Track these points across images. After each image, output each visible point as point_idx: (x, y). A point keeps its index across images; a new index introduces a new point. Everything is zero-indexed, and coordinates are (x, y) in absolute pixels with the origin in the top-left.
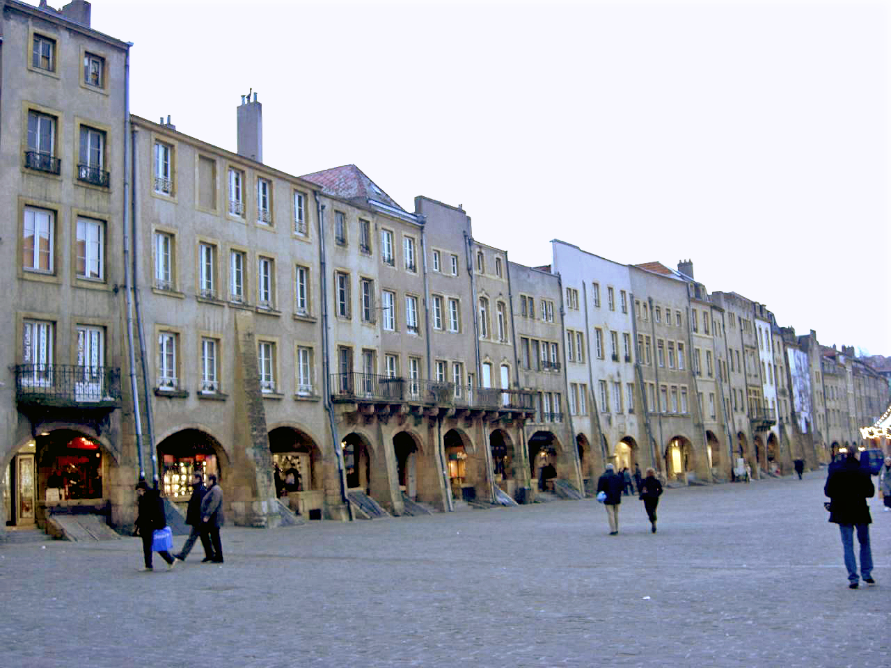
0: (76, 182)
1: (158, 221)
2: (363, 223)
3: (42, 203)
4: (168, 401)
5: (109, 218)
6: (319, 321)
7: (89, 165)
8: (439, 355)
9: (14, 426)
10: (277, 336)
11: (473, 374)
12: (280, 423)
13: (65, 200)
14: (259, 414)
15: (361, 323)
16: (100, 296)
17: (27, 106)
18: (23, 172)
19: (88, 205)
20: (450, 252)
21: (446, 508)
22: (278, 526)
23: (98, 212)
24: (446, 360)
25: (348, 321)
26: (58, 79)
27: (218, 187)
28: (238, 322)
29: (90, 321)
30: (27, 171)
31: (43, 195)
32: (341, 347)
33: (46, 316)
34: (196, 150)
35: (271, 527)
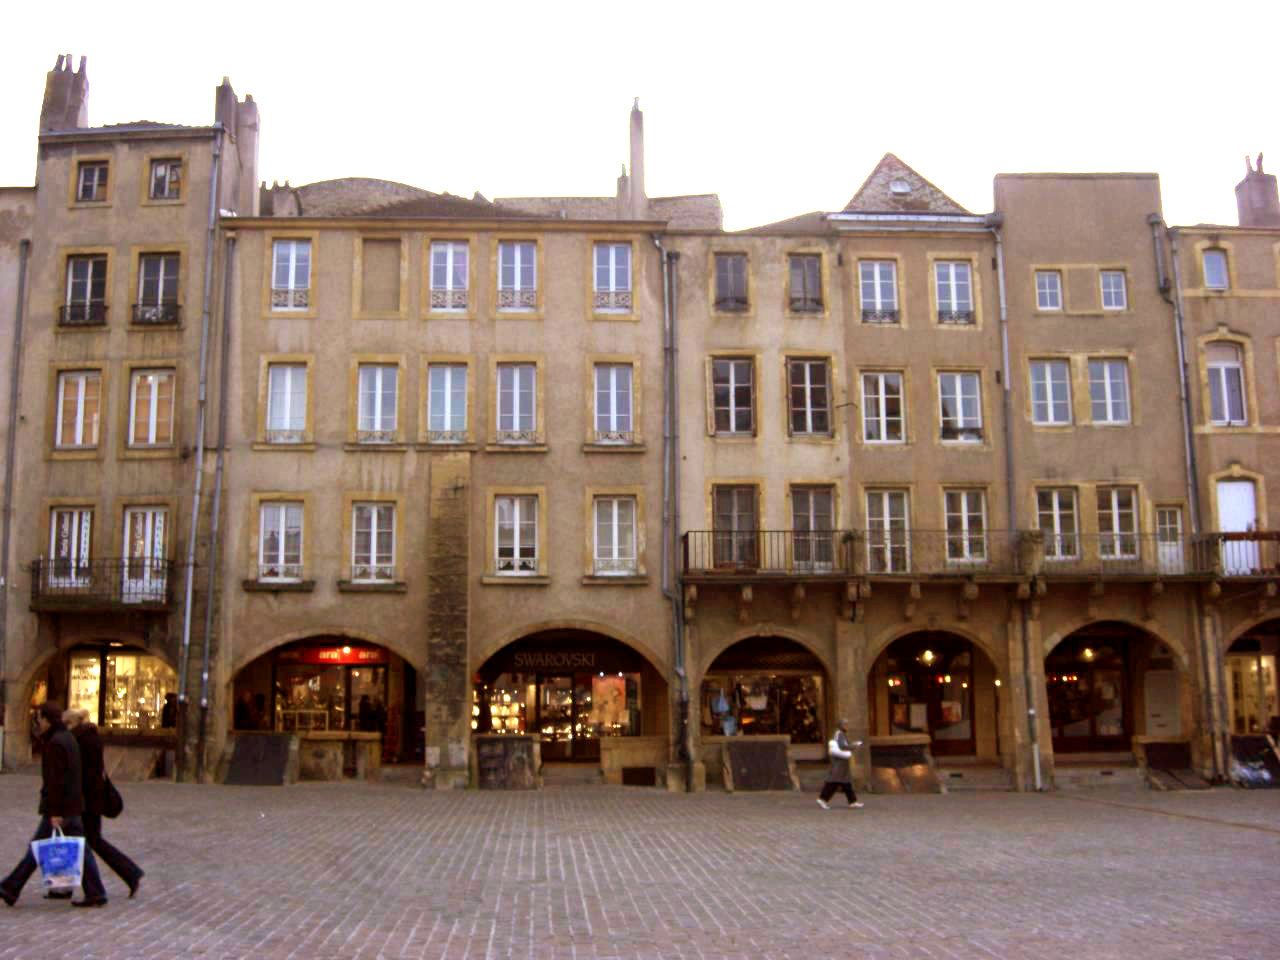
0: (129, 327)
1: (276, 349)
2: (805, 261)
3: (80, 364)
4: (271, 598)
5: (178, 363)
6: (655, 445)
7: (160, 302)
8: (1048, 477)
9: (33, 636)
10: (542, 484)
11: (1181, 506)
12: (545, 623)
13: (113, 354)
14: (453, 608)
15: (787, 439)
16: (160, 468)
17: (64, 253)
18: (57, 333)
19: (148, 352)
20: (1096, 266)
21: (1021, 781)
22: (456, 787)
23: (163, 358)
24: (1073, 483)
25: (750, 440)
26: (110, 207)
27: (404, 276)
28: (433, 470)
29: (143, 499)
30: (62, 330)
31: (83, 353)
32: (793, 486)
33: (81, 500)
34: (356, 233)
35: (439, 787)
